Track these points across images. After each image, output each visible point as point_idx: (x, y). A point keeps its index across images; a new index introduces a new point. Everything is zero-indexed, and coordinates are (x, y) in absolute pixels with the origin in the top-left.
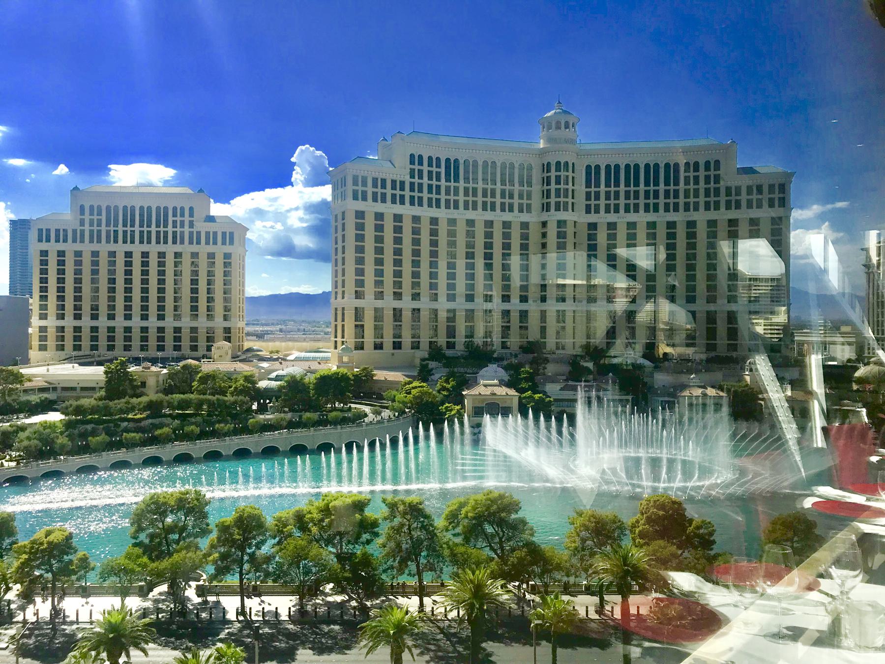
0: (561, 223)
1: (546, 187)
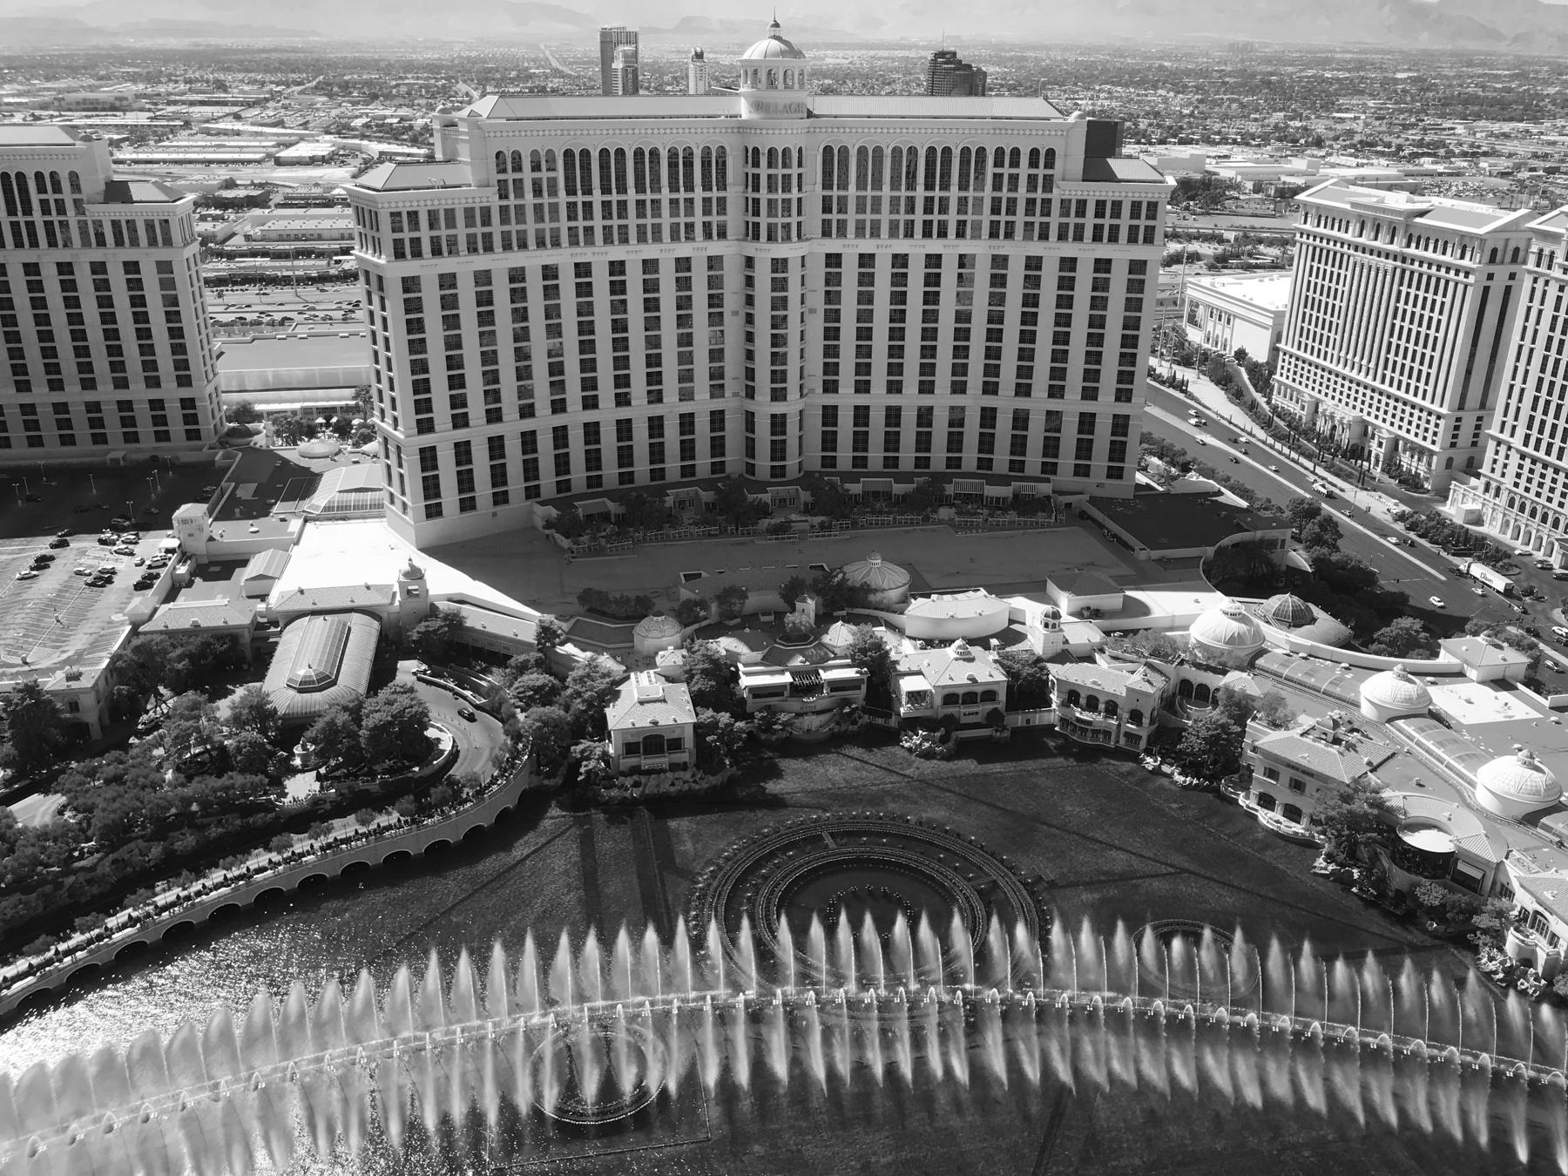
0: (779, 265)
1: (751, 195)
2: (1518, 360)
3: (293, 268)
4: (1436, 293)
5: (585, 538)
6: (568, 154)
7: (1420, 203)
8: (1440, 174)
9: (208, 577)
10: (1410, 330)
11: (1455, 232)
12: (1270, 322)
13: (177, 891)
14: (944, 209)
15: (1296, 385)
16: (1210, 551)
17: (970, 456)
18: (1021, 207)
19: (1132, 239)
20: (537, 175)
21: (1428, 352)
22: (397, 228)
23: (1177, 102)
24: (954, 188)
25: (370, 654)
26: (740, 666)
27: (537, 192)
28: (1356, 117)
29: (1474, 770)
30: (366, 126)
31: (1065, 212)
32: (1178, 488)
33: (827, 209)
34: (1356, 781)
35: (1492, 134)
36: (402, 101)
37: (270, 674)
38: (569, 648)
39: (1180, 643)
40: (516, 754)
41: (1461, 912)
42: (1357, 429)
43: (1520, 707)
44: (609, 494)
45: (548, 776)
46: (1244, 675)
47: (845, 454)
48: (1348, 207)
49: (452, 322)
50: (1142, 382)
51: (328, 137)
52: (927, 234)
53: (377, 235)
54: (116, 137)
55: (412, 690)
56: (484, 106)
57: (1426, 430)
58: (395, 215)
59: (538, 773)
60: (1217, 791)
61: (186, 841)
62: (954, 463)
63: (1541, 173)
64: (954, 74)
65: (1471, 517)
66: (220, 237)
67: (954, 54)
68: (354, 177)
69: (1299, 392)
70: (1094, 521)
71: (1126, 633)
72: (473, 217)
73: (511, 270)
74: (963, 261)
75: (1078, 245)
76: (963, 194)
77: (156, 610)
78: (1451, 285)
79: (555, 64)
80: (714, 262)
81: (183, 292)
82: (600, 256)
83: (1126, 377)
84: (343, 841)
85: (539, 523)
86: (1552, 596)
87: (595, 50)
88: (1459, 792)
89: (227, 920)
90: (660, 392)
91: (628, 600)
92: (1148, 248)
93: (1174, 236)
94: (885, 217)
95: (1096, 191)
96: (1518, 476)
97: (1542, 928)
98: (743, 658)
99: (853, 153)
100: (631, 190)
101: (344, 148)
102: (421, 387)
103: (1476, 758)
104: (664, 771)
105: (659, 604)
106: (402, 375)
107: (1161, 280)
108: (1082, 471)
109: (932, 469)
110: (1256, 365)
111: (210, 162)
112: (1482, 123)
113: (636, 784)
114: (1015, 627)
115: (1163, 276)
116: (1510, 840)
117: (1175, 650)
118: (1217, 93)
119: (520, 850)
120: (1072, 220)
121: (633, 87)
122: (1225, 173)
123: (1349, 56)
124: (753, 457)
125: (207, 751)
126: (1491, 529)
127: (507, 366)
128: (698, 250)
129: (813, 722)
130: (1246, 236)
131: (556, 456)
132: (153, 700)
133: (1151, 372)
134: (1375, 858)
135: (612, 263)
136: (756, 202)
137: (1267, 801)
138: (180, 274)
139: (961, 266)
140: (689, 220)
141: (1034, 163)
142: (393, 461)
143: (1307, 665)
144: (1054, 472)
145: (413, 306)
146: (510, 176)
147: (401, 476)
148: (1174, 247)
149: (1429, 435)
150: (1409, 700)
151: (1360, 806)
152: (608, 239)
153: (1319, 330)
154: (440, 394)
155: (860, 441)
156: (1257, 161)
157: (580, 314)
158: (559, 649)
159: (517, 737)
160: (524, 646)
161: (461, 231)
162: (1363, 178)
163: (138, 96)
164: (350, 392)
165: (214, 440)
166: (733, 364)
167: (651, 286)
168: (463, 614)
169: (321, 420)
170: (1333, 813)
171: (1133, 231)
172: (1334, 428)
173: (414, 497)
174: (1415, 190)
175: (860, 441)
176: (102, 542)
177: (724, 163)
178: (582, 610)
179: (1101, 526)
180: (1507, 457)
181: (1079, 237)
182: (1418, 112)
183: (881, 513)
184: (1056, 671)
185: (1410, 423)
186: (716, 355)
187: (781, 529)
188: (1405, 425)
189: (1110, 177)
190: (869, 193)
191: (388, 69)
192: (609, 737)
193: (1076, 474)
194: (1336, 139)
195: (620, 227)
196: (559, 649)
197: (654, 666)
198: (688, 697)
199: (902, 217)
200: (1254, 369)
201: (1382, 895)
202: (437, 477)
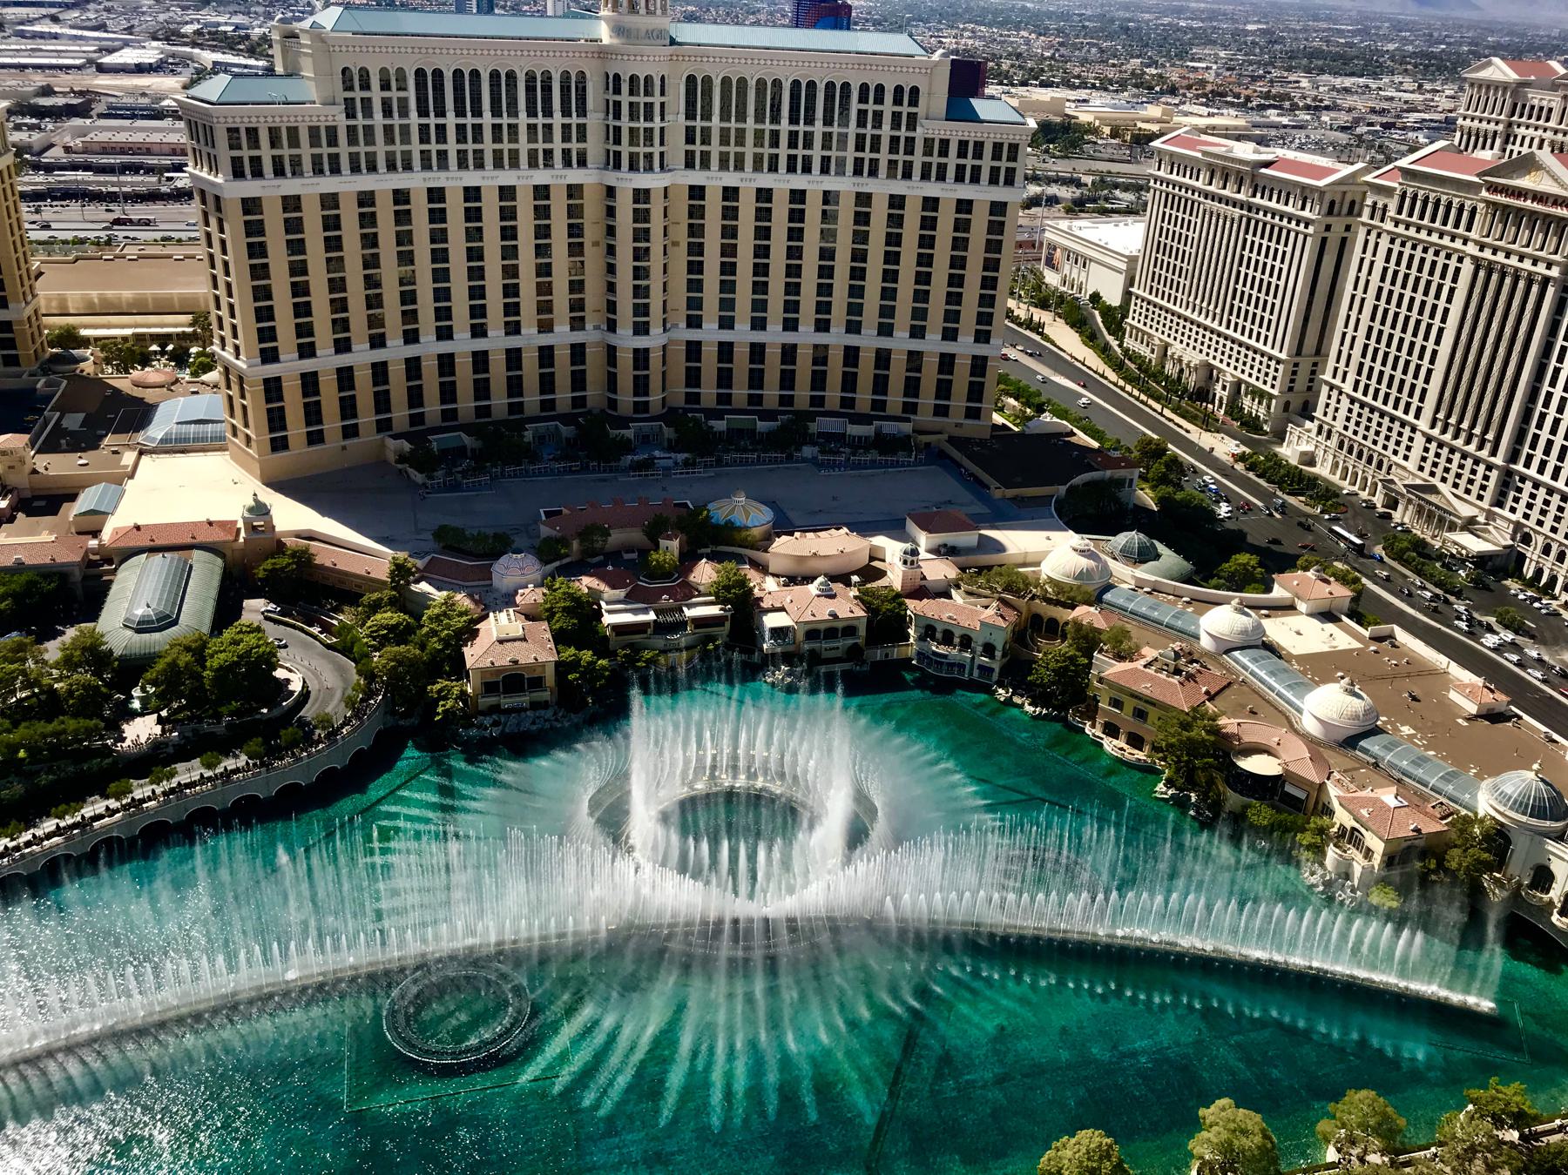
0: (641, 195)
1: (612, 123)
2: (1350, 308)
3: (120, 184)
4: (1278, 242)
5: (440, 473)
6: (420, 73)
7: (1267, 154)
8: (1285, 127)
9: (32, 512)
11: (1296, 184)
12: (1124, 267)
14: (808, 144)
15: (1147, 329)
16: (1062, 489)
18: (885, 144)
19: (994, 181)
20: (386, 94)
22: (234, 145)
23: (1039, 45)
24: (819, 123)
25: (214, 593)
26: (603, 604)
27: (387, 113)
28: (1209, 66)
29: (1301, 697)
30: (198, 33)
31: (928, 151)
32: (1033, 428)
33: (690, 139)
34: (1194, 709)
35: (1334, 88)
36: (237, 8)
37: (104, 614)
38: (424, 587)
42: (1203, 373)
43: (1341, 638)
44: (467, 428)
45: (404, 716)
46: (1092, 609)
47: (709, 391)
48: (1199, 155)
49: (296, 247)
50: (1000, 323)
51: (155, 44)
52: (791, 169)
55: (258, 629)
57: (1267, 374)
58: (233, 131)
59: (393, 713)
60: (1064, 720)
62: (817, 401)
63: (1378, 128)
65: (1306, 458)
66: (36, 148)
69: (1150, 336)
70: (953, 461)
71: (982, 569)
73: (360, 193)
75: (940, 185)
76: (828, 129)
78: (1292, 235)
80: (574, 191)
82: (454, 180)
83: (985, 319)
84: (189, 786)
85: (392, 457)
86: (1375, 533)
88: (1287, 718)
91: (487, 537)
92: (1008, 189)
93: (1034, 179)
94: (749, 150)
95: (957, 131)
96: (1348, 419)
98: (605, 596)
99: (717, 83)
101: (173, 56)
102: (264, 314)
103: (1302, 688)
104: (525, 710)
105: (519, 541)
107: (1021, 222)
108: (941, 411)
110: (1109, 308)
111: (23, 67)
112: (1326, 77)
113: (495, 724)
114: (876, 564)
115: (1023, 217)
116: (1331, 762)
118: (1077, 37)
119: (376, 790)
120: (935, 159)
122: (1085, 117)
124: (615, 392)
126: (1322, 470)
127: (356, 292)
128: (558, 177)
130: (1102, 181)
131: (409, 388)
133: (1009, 314)
134: (1211, 782)
136: (618, 130)
137: (1112, 730)
139: (826, 202)
141: (898, 101)
142: (234, 392)
144: (915, 413)
145: (254, 228)
146: (358, 94)
147: (244, 408)
148: (1034, 189)
150: (1244, 632)
151: (1198, 733)
153: (1169, 275)
154: (285, 323)
155: (725, 378)
156: (1114, 106)
157: (433, 241)
158: (414, 587)
159: (370, 676)
160: (377, 584)
161: (306, 151)
162: (1214, 128)
165: (35, 367)
166: (593, 296)
167: (508, 214)
168: (312, 551)
169: (154, 348)
172: (1181, 371)
173: (257, 429)
174: (1262, 141)
175: (725, 378)
177: (584, 89)
179: (959, 465)
180: (1338, 401)
181: (941, 177)
182: (1266, 65)
183: (745, 450)
184: (913, 606)
185: (1252, 367)
186: (576, 286)
187: (648, 464)
188: (1247, 369)
189: (974, 118)
190: (733, 124)
192: (468, 677)
194: (1189, 87)
195: (475, 151)
196: (414, 587)
197: (512, 603)
198: (549, 635)
199: (767, 151)
200: (1107, 312)
202: (282, 408)
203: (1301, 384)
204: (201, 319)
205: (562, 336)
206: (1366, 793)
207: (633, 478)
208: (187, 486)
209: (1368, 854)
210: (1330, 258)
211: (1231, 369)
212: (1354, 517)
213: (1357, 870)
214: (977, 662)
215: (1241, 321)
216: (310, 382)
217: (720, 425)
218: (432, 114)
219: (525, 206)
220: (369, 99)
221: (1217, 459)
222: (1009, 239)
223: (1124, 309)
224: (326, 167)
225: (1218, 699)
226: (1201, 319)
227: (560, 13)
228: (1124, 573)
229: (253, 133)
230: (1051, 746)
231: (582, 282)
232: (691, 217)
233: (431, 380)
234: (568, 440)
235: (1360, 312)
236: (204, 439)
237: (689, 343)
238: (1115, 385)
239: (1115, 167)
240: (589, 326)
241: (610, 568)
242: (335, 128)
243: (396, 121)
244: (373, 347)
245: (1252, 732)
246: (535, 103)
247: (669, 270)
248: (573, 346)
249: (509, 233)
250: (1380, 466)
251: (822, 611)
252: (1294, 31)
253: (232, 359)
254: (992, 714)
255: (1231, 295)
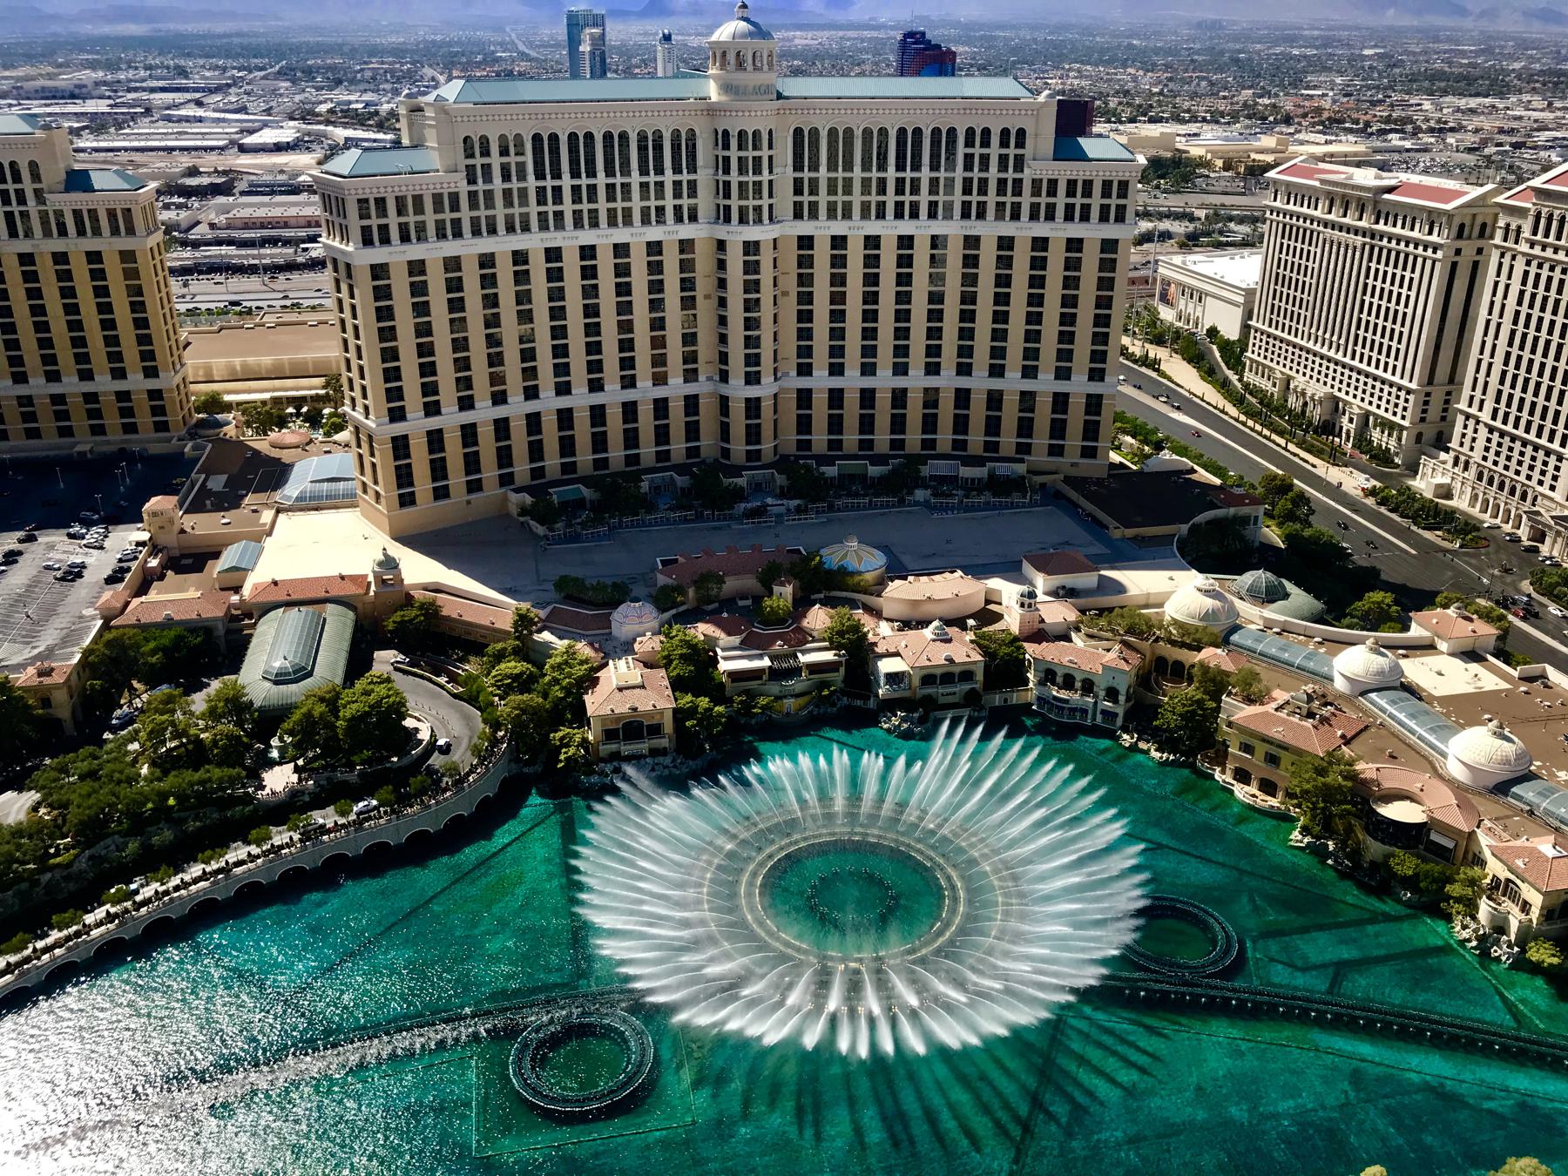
0: (751, 247)
1: (722, 178)
2: (1486, 334)
3: (260, 257)
4: (1404, 269)
6: (537, 138)
7: (1389, 180)
8: (1408, 150)
9: (180, 570)
10: (1379, 306)
11: (1423, 208)
12: (1241, 300)
13: (155, 886)
14: (915, 190)
15: (1267, 362)
16: (1184, 528)
17: (945, 437)
18: (992, 187)
20: (505, 160)
21: (1397, 327)
23: (1147, 81)
25: (346, 645)
27: (506, 177)
28: (1324, 93)
29: (1445, 741)
30: (331, 111)
31: (1036, 191)
32: (1152, 465)
33: (798, 190)
34: (1329, 754)
35: (1458, 110)
36: (367, 86)
38: (546, 636)
39: (1154, 622)
40: (495, 742)
41: (1434, 881)
42: (1328, 406)
43: (1487, 679)
44: (584, 480)
45: (527, 763)
46: (1219, 651)
47: (820, 437)
48: (1317, 184)
51: (292, 123)
52: (899, 215)
53: (344, 222)
54: (76, 125)
55: (388, 680)
56: (451, 90)
57: (1396, 405)
58: (363, 202)
59: (518, 760)
60: (1193, 767)
61: (163, 836)
62: (929, 444)
63: (1507, 148)
64: (923, 55)
66: (184, 226)
67: (923, 34)
68: (320, 163)
69: (1271, 369)
71: (1102, 611)
72: (442, 203)
73: (481, 256)
74: (936, 242)
75: (1050, 225)
76: (935, 175)
77: (127, 604)
78: (1420, 260)
79: (522, 47)
80: (686, 246)
81: (147, 280)
82: (570, 240)
83: (1099, 357)
85: (514, 510)
86: (1521, 569)
87: (561, 32)
88: (1431, 763)
89: (206, 914)
90: (633, 376)
91: (605, 586)
93: (1146, 215)
94: (857, 199)
96: (1487, 449)
97: (1514, 896)
98: (721, 643)
99: (824, 134)
100: (601, 174)
101: (309, 134)
102: (392, 375)
104: (645, 757)
105: (637, 590)
106: (372, 362)
108: (1055, 451)
109: (908, 450)
110: (1228, 342)
111: (171, 149)
112: (1449, 99)
115: (1135, 255)
116: (1481, 809)
117: (1150, 627)
118: (1186, 71)
119: (502, 836)
120: (1044, 200)
121: (601, 69)
122: (1196, 152)
123: (1316, 33)
125: (182, 744)
126: (1460, 503)
127: (478, 352)
128: (669, 233)
129: (790, 704)
130: (1216, 214)
132: (126, 694)
133: (1124, 352)
134: (1349, 830)
135: (582, 248)
136: (727, 184)
137: (1243, 776)
138: (144, 264)
139: (934, 246)
140: (660, 203)
141: (1004, 143)
142: (365, 450)
143: (1281, 641)
144: (1029, 453)
145: (382, 293)
146: (478, 161)
147: (374, 465)
148: (1145, 226)
149: (1399, 410)
150: (1381, 673)
151: (1334, 778)
152: (578, 224)
153: (1289, 307)
154: (411, 382)
155: (835, 424)
156: (1226, 139)
157: (551, 299)
158: (536, 637)
159: (496, 725)
160: (501, 635)
161: (430, 218)
162: (1332, 155)
163: (97, 84)
164: (320, 381)
166: (706, 348)
167: (622, 270)
169: (291, 410)
170: (1307, 786)
171: (1104, 210)
172: (1305, 404)
173: (386, 485)
174: (1383, 167)
175: (835, 424)
176: (71, 536)
177: (694, 146)
178: (557, 596)
179: (1077, 506)
180: (1476, 431)
182: (1385, 89)
183: (857, 495)
184: (1032, 650)
186: (689, 339)
187: (761, 512)
188: (1375, 400)
189: (1082, 157)
190: (840, 174)
191: (353, 52)
193: (1050, 454)
194: (1305, 116)
196: (536, 637)
197: (633, 652)
198: (667, 683)
199: (874, 198)
200: (1226, 346)
201: (1357, 865)
202: (409, 465)
203: (1434, 411)
204: (333, 381)
205: (676, 388)
206: (1521, 842)
207: (747, 525)
208: (322, 541)
209: (1525, 907)
210: (1462, 282)
211: (1358, 401)
212: (1497, 552)
213: (1514, 926)
214: (1100, 707)
215: (1366, 351)
216: (435, 440)
217: (831, 471)
218: (549, 177)
219: (638, 262)
220: (489, 165)
221: (1346, 494)
222: (1121, 277)
223: (1243, 342)
224: (449, 232)
225: (1355, 744)
226: (1317, 348)
227: (670, 74)
228: (1249, 611)
229: (381, 202)
230: (1179, 793)
231: (695, 334)
232: (800, 266)
233: (550, 434)
234: (682, 489)
235: (1496, 337)
236: (336, 497)
237: (799, 391)
238: (1237, 420)
239: (1228, 200)
240: (702, 378)
241: (725, 615)
242: (457, 194)
243: (515, 185)
244: (495, 403)
245: (1392, 777)
246: (647, 161)
247: (780, 319)
248: (687, 398)
249: (623, 289)
250: (1524, 497)
251: (938, 655)
252: (1414, 54)
253: (361, 418)
254: (1118, 759)
255: (1357, 326)
